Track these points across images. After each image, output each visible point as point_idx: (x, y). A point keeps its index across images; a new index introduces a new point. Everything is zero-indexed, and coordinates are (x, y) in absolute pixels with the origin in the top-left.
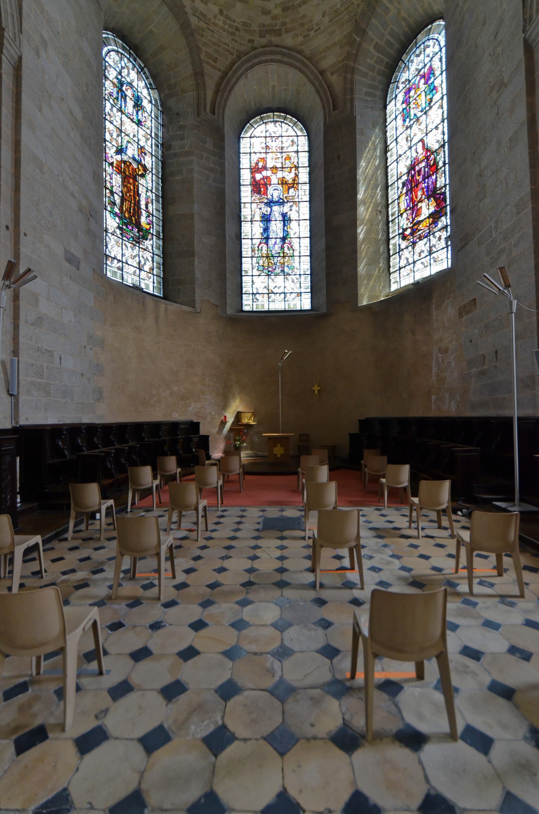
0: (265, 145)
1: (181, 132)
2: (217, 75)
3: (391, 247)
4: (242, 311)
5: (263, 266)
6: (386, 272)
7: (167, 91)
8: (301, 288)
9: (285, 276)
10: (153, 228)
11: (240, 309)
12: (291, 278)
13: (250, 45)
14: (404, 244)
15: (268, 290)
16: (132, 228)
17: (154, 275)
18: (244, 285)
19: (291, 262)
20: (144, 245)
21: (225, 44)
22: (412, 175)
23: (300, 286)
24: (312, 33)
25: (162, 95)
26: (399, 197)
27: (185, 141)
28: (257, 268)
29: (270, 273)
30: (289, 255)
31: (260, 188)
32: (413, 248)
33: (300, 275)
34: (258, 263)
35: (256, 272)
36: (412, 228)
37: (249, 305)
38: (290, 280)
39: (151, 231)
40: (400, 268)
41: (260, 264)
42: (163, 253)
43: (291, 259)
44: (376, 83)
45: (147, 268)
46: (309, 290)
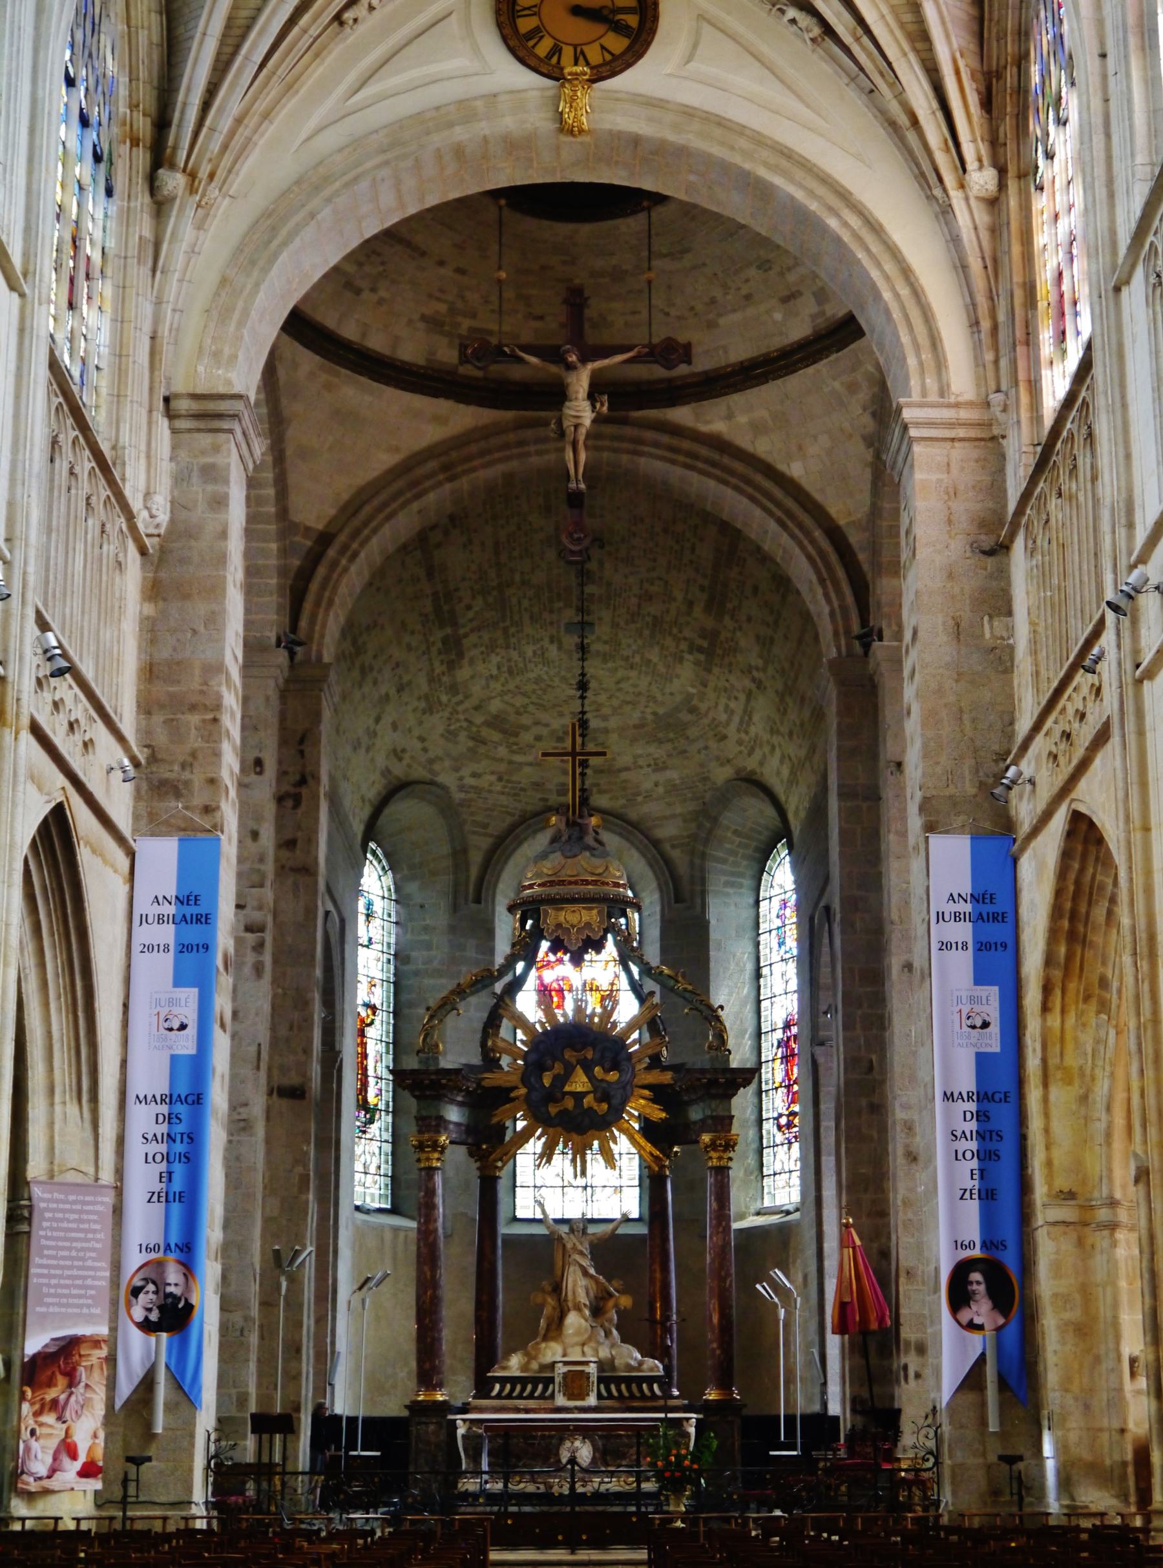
1: (427, 937)
2: (485, 843)
3: (764, 1132)
4: (515, 1219)
6: (756, 1173)
7: (406, 872)
11: (511, 1215)
13: (542, 803)
14: (779, 1138)
21: (502, 806)
24: (640, 799)
25: (398, 876)
26: (773, 1060)
27: (434, 953)
31: (551, 997)
36: (788, 1116)
40: (775, 1174)
42: (393, 1135)
44: (741, 869)
46: (636, 1182)
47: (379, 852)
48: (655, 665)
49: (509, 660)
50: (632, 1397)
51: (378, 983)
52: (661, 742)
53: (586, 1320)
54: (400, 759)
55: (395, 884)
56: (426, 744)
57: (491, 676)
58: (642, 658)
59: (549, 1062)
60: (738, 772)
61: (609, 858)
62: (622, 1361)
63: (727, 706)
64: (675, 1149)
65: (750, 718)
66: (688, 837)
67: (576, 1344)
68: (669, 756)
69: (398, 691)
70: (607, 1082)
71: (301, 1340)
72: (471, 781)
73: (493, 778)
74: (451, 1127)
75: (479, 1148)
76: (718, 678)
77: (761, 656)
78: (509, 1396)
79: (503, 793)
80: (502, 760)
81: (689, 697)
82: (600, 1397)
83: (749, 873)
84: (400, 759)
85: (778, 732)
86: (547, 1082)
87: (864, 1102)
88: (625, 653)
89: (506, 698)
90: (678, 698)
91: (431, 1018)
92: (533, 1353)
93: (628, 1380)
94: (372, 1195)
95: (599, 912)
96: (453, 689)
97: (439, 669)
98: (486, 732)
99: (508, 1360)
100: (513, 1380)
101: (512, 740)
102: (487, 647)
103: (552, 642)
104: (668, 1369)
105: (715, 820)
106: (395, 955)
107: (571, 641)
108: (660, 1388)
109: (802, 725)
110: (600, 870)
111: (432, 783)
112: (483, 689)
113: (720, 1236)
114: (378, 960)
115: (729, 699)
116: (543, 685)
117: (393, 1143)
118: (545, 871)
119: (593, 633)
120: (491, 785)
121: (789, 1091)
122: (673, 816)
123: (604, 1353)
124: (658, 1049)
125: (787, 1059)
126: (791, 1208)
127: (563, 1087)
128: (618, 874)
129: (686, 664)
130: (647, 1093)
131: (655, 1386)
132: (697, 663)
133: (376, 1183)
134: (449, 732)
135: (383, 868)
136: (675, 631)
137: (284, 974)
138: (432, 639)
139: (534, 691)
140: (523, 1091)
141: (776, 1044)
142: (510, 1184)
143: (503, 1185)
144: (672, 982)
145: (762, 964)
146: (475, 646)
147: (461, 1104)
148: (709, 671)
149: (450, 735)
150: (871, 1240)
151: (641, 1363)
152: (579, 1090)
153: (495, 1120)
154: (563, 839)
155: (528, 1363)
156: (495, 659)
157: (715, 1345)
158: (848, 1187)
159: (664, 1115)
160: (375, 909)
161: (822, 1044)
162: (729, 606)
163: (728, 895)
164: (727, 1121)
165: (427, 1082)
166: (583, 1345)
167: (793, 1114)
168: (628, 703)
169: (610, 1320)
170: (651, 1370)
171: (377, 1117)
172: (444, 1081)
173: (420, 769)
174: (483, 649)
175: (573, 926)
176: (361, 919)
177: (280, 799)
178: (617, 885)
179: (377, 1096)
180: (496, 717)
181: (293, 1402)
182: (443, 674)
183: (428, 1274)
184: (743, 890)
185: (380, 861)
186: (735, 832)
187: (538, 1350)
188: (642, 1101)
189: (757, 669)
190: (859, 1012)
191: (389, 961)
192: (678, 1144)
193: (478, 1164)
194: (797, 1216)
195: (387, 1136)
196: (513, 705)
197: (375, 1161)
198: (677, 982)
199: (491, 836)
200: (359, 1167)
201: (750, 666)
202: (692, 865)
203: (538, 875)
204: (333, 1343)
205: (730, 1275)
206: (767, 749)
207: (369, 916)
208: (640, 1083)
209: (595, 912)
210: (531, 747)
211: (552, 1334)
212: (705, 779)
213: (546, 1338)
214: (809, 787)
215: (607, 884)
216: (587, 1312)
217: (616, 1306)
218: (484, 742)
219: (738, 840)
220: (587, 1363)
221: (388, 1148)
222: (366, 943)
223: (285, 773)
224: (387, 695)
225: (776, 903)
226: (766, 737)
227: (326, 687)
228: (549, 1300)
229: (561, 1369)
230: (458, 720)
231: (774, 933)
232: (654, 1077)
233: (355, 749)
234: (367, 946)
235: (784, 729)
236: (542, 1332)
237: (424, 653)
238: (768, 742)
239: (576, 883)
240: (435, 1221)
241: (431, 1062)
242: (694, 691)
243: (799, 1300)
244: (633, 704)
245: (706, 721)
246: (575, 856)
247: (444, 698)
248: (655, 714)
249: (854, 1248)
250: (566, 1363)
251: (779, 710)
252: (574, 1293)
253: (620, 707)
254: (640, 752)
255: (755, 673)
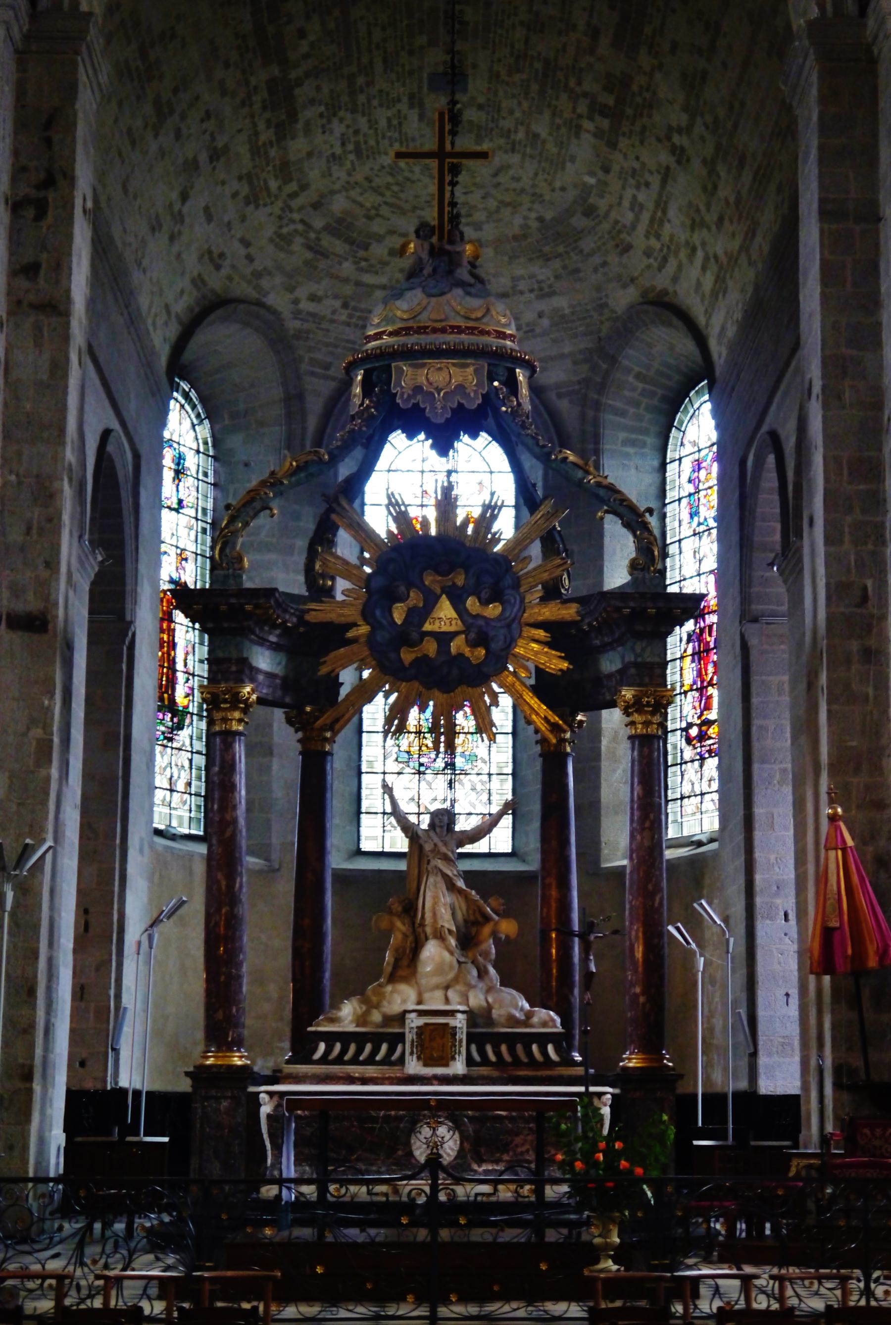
0: (420, 490)
3: (669, 747)
4: (359, 853)
5: (408, 752)
7: (227, 422)
8: (490, 803)
9: (457, 777)
10: (193, 701)
11: (355, 848)
12: (470, 780)
14: (689, 753)
15: (419, 806)
16: (164, 715)
17: (191, 794)
18: (364, 792)
19: (470, 745)
20: (178, 741)
21: (348, 341)
22: (700, 628)
23: (489, 799)
25: (217, 427)
26: (682, 658)
28: (395, 756)
29: (422, 769)
30: (466, 730)
32: (701, 766)
33: (490, 775)
34: (399, 746)
35: (392, 766)
36: (700, 726)
37: (375, 838)
38: (468, 786)
39: (190, 710)
40: (682, 798)
41: (401, 749)
43: (470, 739)
44: (644, 424)
45: (180, 786)
47: (193, 394)
48: (544, 142)
49: (357, 132)
50: (517, 1062)
51: (191, 557)
52: (547, 258)
53: (452, 953)
54: (218, 267)
55: (213, 436)
56: (251, 250)
57: (333, 155)
58: (527, 133)
59: (402, 589)
60: (644, 294)
61: (492, 299)
62: (503, 1012)
63: (634, 197)
64: (579, 718)
65: (664, 212)
66: (579, 382)
67: (437, 987)
68: (557, 277)
69: (211, 159)
70: (484, 618)
71: (36, 976)
72: (311, 307)
73: (337, 304)
74: (261, 677)
75: (301, 711)
76: (625, 155)
77: (686, 109)
78: (339, 1060)
79: (348, 325)
80: (346, 280)
81: (586, 190)
82: (470, 1062)
83: (654, 429)
84: (218, 267)
85: (703, 224)
86: (399, 615)
87: (855, 646)
88: (507, 123)
89: (352, 193)
90: (572, 194)
91: (232, 520)
92: (374, 999)
93: (511, 1040)
94: (180, 818)
95: (476, 371)
96: (285, 171)
97: (266, 135)
98: (327, 241)
99: (339, 1009)
100: (345, 1038)
101: (361, 253)
102: (327, 105)
103: (411, 106)
104: (567, 1022)
105: (613, 360)
106: (213, 524)
107: (437, 102)
108: (557, 1050)
109: (738, 201)
110: (479, 314)
111: (259, 304)
112: (323, 176)
113: (646, 833)
114: (191, 529)
115: (638, 187)
116: (400, 178)
117: (207, 755)
118: (399, 313)
119: (465, 90)
120: (334, 312)
121: (701, 695)
122: (562, 356)
123: (477, 999)
124: (558, 572)
125: (700, 656)
126: (704, 838)
127: (422, 625)
128: (503, 320)
129: (586, 137)
130: (541, 634)
131: (550, 1048)
132: (598, 134)
133: (185, 803)
134: (280, 236)
135: (198, 416)
136: (572, 82)
137: (19, 454)
138: (253, 81)
139: (388, 186)
140: (364, 629)
141: (685, 638)
142: (354, 809)
143: (337, 764)
144: (580, 474)
145: (668, 541)
146: (312, 102)
147: (275, 648)
148: (613, 145)
149: (282, 241)
150: (865, 844)
151: (529, 1015)
152: (445, 629)
153: (324, 670)
154: (425, 272)
155: (367, 1013)
156: (338, 128)
157: (638, 990)
158: (831, 766)
159: (565, 665)
160: (187, 464)
161: (755, 620)
162: (648, 30)
163: (627, 455)
164: (658, 671)
165: (223, 608)
166: (447, 988)
167: (709, 723)
168: (508, 204)
169: (486, 955)
170: (544, 1024)
171: (187, 721)
172: (248, 607)
173: (244, 285)
174: (322, 109)
175: (439, 390)
176: (168, 475)
177: (16, 207)
178: (502, 335)
179: (187, 696)
180: (340, 221)
181: (23, 1066)
182: (271, 143)
183: (224, 883)
184: (646, 450)
185: (194, 407)
186: (638, 376)
187: (381, 996)
188: (535, 646)
189: (680, 131)
190: (849, 519)
191: (204, 531)
192: (583, 710)
193: (300, 735)
194: (714, 846)
195: (200, 746)
196: (361, 205)
197: (185, 776)
198: (588, 473)
199: (334, 379)
200: (161, 781)
201: (670, 128)
202: (583, 416)
203: (387, 320)
204: (118, 996)
205: (661, 890)
206: (683, 255)
207: (179, 473)
208: (532, 621)
209: (471, 370)
210: (386, 264)
211: (400, 973)
212: (602, 306)
213: (393, 978)
214: (742, 291)
215: (488, 333)
216: (453, 942)
217: (494, 934)
218: (325, 255)
219: (640, 386)
220: (452, 1013)
221: (200, 761)
222: (175, 506)
223: (24, 169)
224: (195, 161)
225: (687, 464)
226: (683, 236)
227: (84, 49)
228: (399, 924)
229: (414, 1022)
230: (292, 221)
231: (684, 502)
232: (551, 612)
233: (153, 229)
234: (177, 510)
235: (711, 218)
236: (387, 968)
237: (243, 104)
238: (687, 243)
239: (443, 331)
240: (234, 808)
241: (231, 581)
242: (592, 181)
243: (732, 940)
244: (514, 206)
245: (606, 226)
246: (442, 294)
247: (273, 185)
248: (540, 219)
249: (844, 850)
250: (421, 1013)
251: (705, 189)
252: (434, 914)
253: (498, 211)
254: (520, 272)
255: (676, 139)
